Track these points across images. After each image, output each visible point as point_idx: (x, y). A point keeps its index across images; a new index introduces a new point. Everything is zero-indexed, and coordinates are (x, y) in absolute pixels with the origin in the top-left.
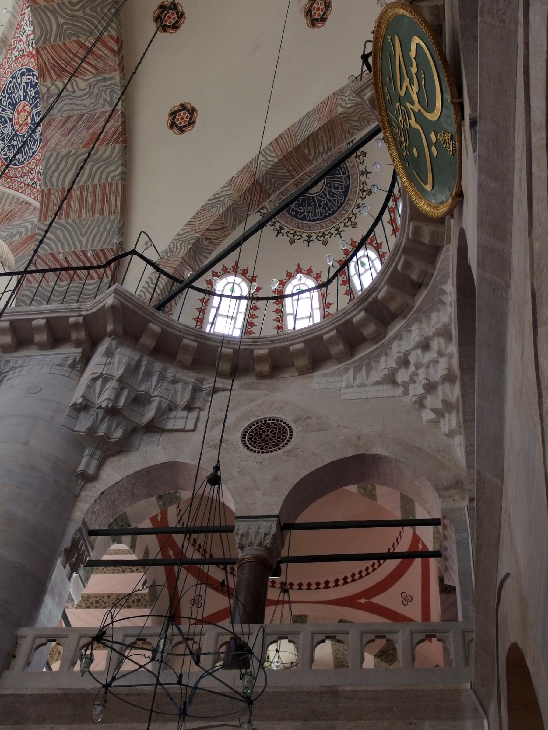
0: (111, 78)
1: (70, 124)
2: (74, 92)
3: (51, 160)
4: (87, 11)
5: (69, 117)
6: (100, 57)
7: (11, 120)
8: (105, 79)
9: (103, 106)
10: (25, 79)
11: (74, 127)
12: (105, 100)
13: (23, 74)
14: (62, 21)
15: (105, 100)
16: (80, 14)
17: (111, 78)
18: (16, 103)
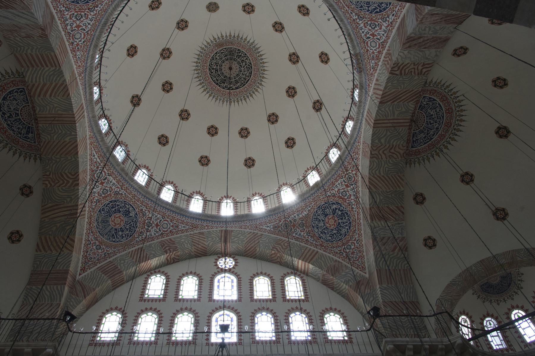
0: (402, 223)
1: (384, 241)
2: (385, 227)
3: (378, 256)
4: (393, 195)
5: (384, 238)
6: (397, 214)
7: (323, 221)
8: (399, 224)
9: (398, 234)
10: (334, 206)
11: (386, 242)
12: (399, 232)
13: (334, 203)
14: (382, 198)
15: (399, 232)
16: (390, 196)
17: (402, 223)
18: (327, 215)
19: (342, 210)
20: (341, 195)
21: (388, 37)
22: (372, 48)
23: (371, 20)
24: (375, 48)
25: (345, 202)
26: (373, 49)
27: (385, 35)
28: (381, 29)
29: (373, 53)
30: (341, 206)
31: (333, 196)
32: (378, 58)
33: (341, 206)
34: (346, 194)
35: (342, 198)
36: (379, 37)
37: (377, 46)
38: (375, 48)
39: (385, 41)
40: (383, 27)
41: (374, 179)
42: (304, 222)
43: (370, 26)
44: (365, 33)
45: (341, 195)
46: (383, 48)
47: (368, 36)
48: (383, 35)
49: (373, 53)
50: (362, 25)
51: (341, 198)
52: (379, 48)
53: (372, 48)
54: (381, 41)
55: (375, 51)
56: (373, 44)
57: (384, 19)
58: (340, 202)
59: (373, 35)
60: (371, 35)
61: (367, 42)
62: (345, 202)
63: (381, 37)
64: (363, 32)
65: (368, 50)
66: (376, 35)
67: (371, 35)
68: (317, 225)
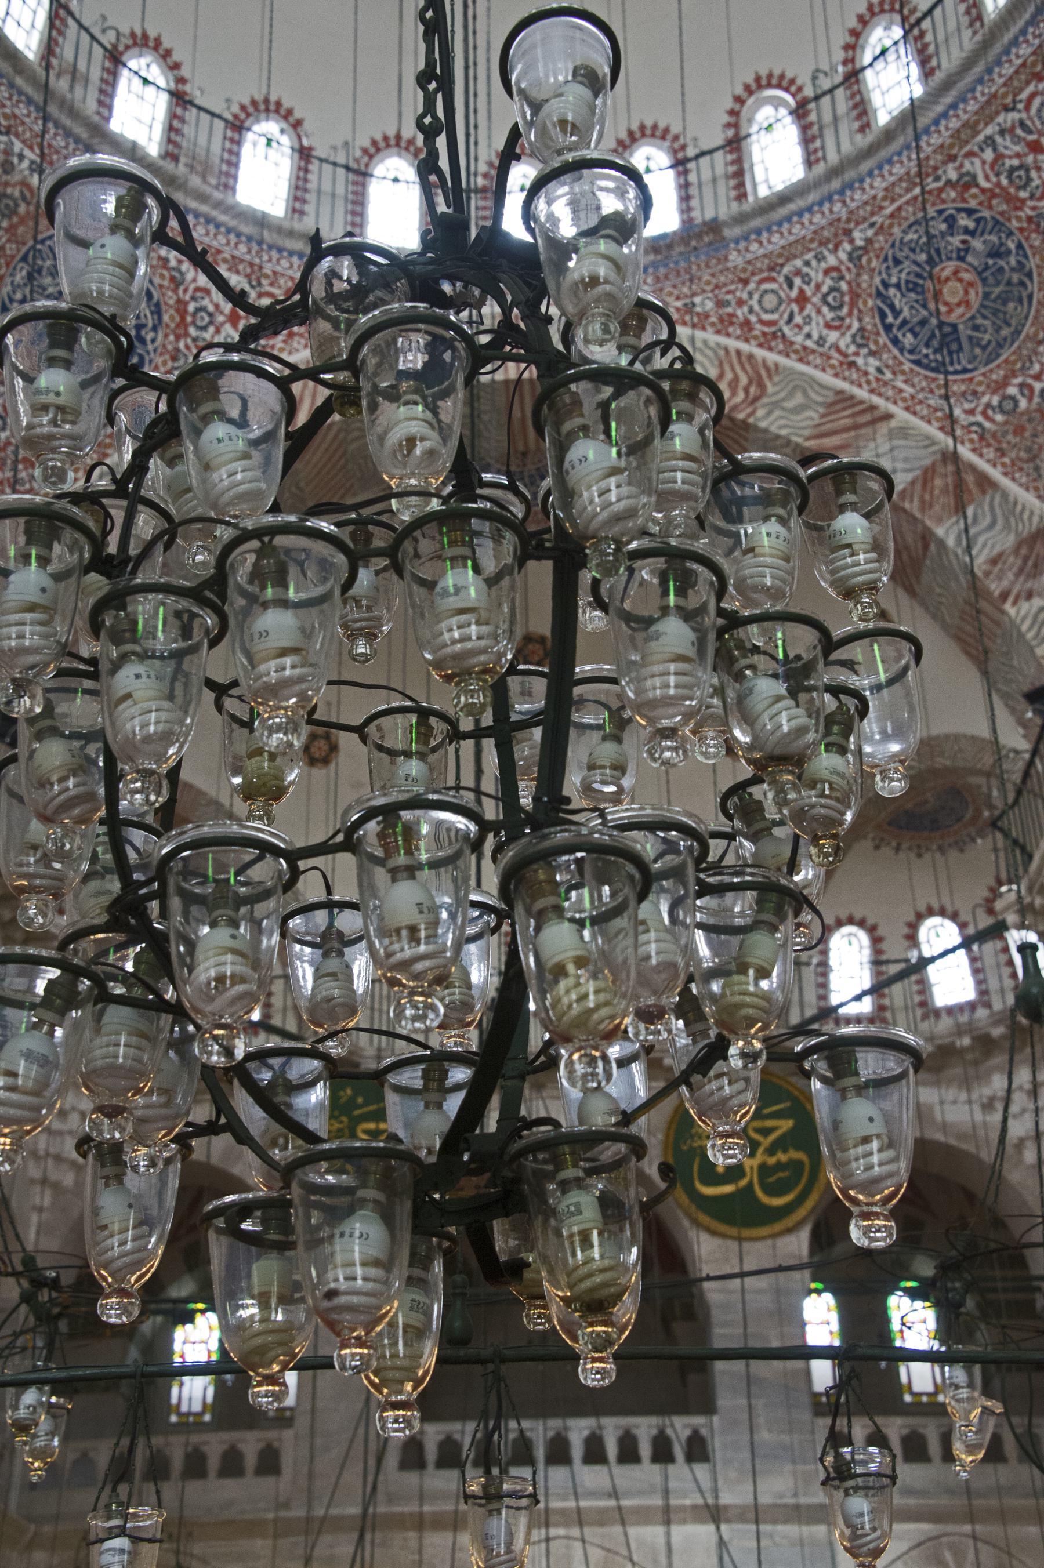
19: (143, 341)
20: (191, 307)
21: (803, 355)
22: (756, 297)
23: (855, 296)
24: (756, 308)
25: (178, 338)
26: (759, 302)
27: (809, 343)
28: (828, 326)
29: (740, 303)
30: (155, 329)
31: (172, 279)
32: (724, 324)
33: (155, 329)
34: (204, 328)
35: (183, 319)
36: (798, 319)
37: (766, 317)
38: (756, 308)
39: (788, 348)
40: (833, 336)
41: (330, 437)
42: (22, 209)
43: (832, 289)
44: (805, 270)
45: (191, 307)
46: (766, 341)
47: (797, 281)
48: (809, 336)
49: (740, 303)
50: (832, 261)
51: (183, 312)
52: (761, 322)
53: (756, 297)
54: (786, 330)
55: (746, 309)
56: (770, 301)
57: (862, 338)
58: (166, 318)
59: (802, 300)
60: (802, 291)
61: (773, 280)
62: (178, 338)
63: (798, 326)
64: (807, 264)
65: (745, 282)
66: (802, 309)
67: (802, 291)
68: (39, 272)
